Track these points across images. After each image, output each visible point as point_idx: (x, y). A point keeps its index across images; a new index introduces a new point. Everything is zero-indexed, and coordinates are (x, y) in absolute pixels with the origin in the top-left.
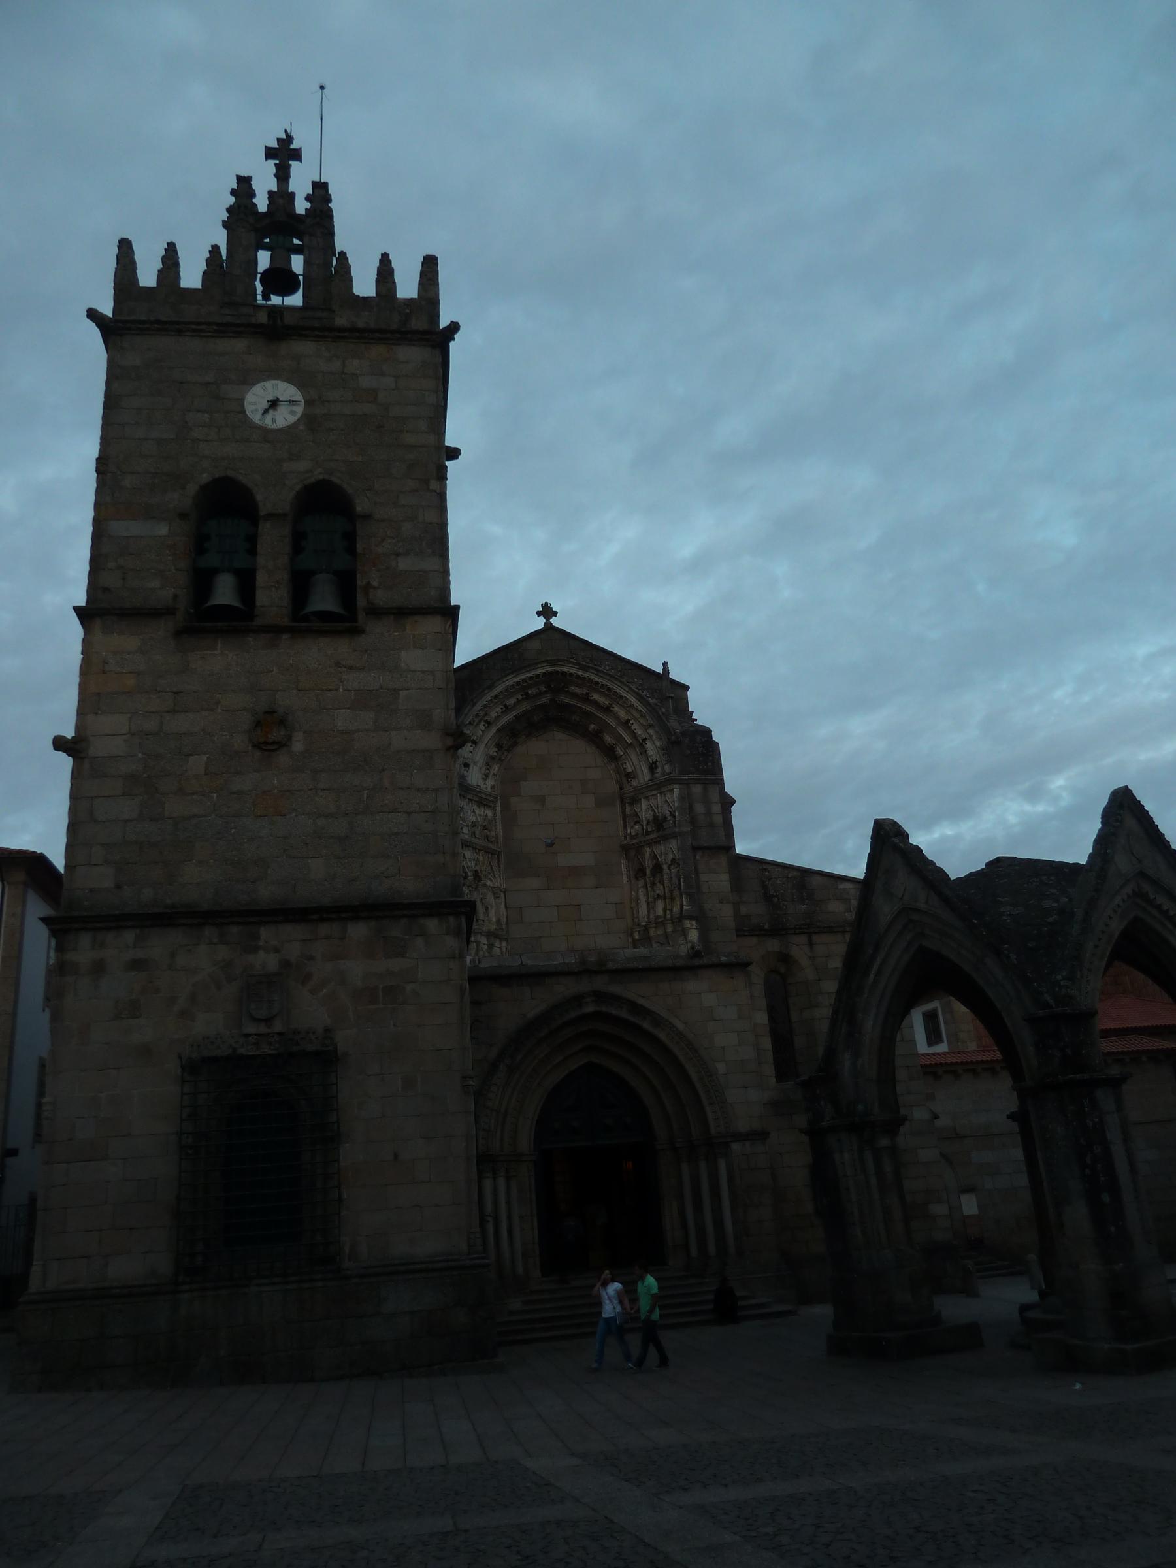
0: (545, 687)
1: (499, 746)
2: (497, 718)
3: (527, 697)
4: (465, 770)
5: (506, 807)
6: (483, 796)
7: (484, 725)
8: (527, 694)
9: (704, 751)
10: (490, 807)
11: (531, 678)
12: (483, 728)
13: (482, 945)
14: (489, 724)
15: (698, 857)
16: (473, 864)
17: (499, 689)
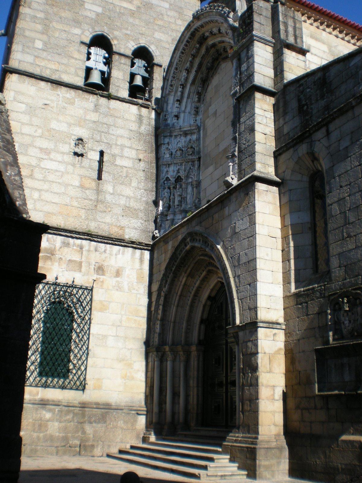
0: (198, 44)
1: (199, 94)
2: (186, 79)
3: (194, 56)
4: (175, 119)
5: (204, 129)
6: (185, 129)
7: (180, 88)
8: (192, 55)
9: (249, 21)
10: (194, 133)
11: (186, 45)
12: (180, 89)
13: (176, 221)
14: (183, 86)
15: (241, 106)
16: (176, 172)
17: (175, 63)
